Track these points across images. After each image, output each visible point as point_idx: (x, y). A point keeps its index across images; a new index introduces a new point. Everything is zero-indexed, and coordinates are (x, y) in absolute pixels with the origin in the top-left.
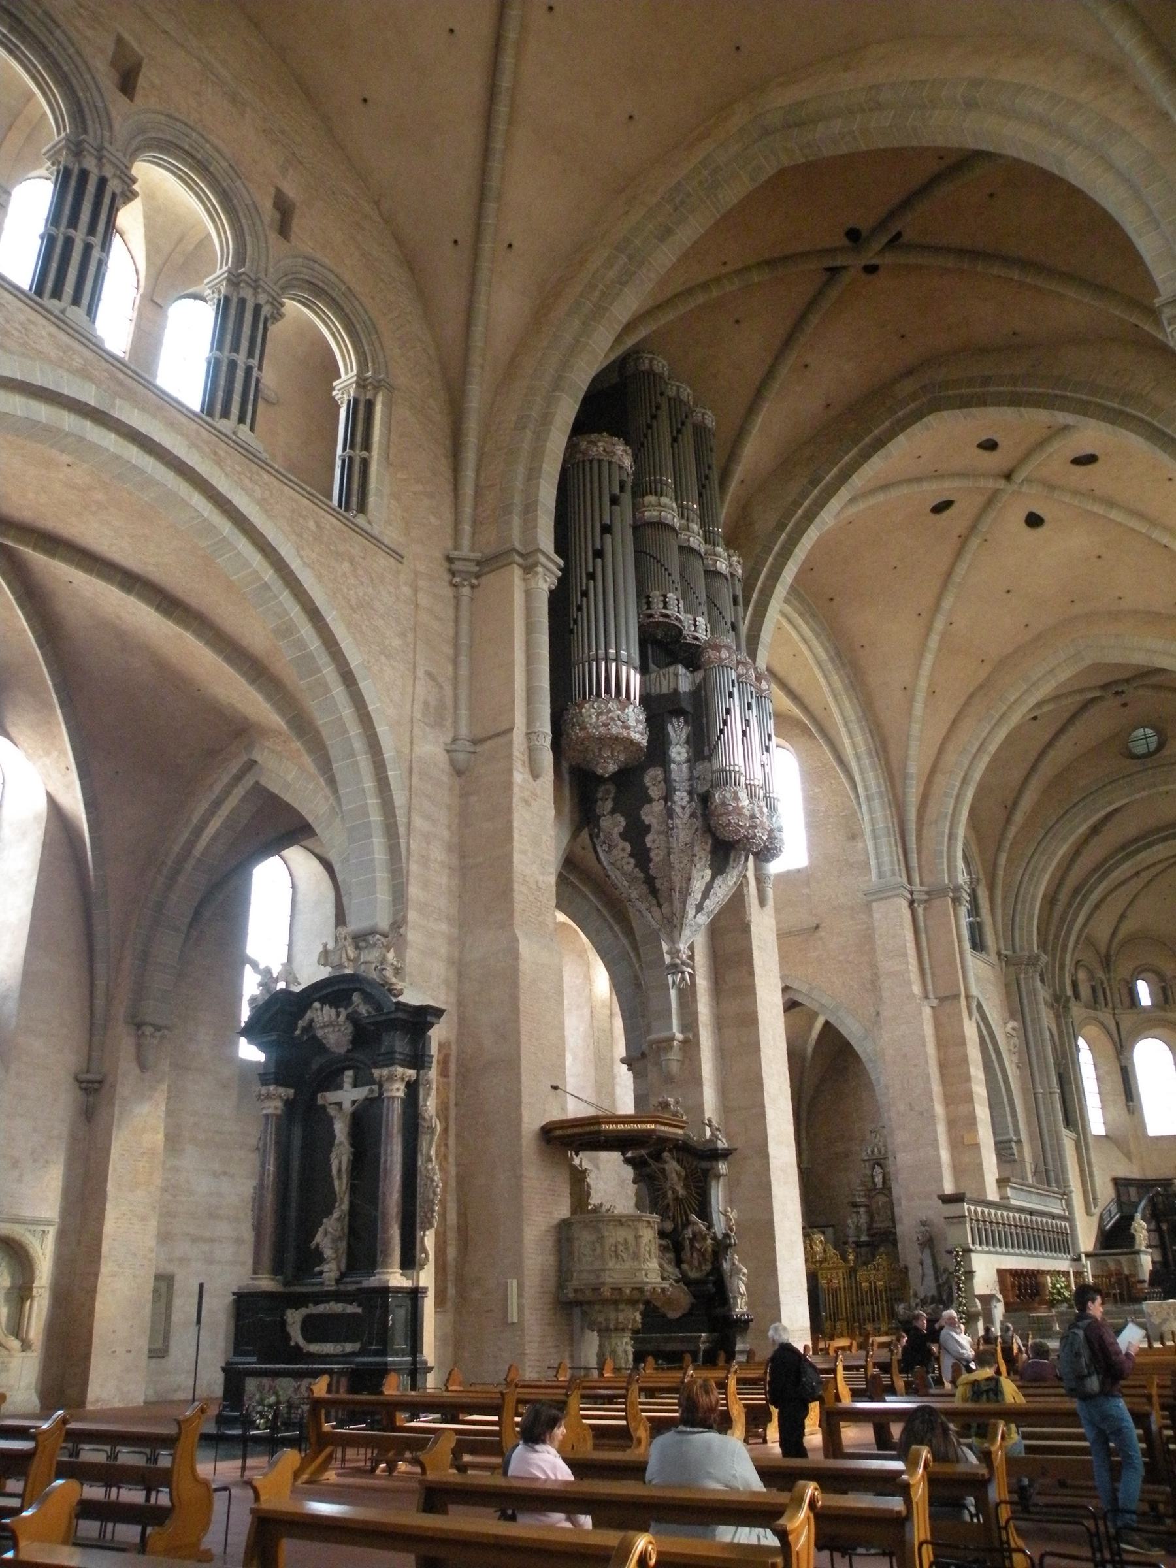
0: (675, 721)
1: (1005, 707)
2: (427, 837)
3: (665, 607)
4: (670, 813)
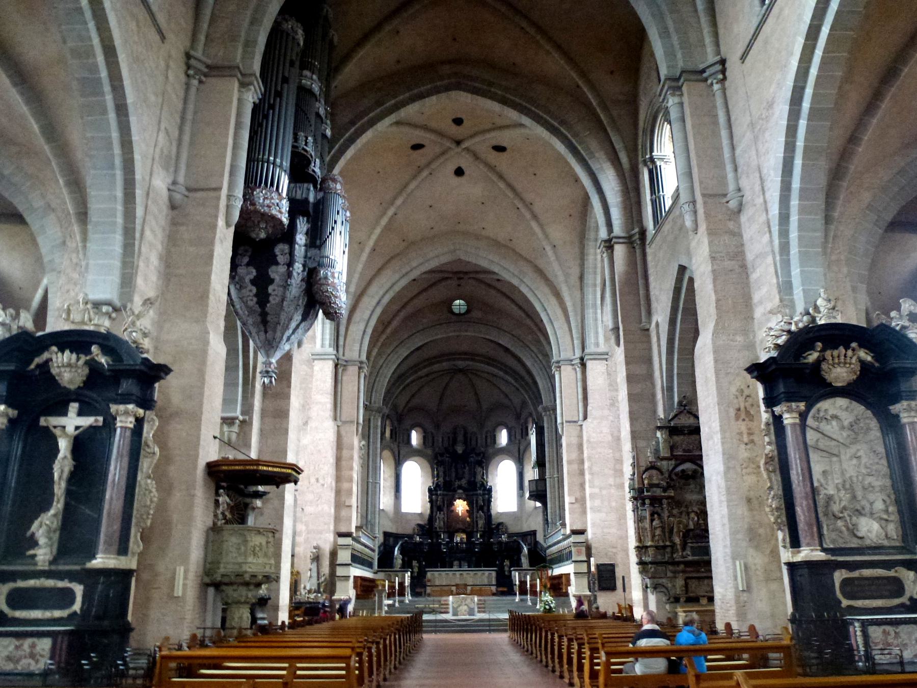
0: (301, 218)
1: (409, 269)
2: (151, 245)
3: (306, 145)
4: (289, 275)
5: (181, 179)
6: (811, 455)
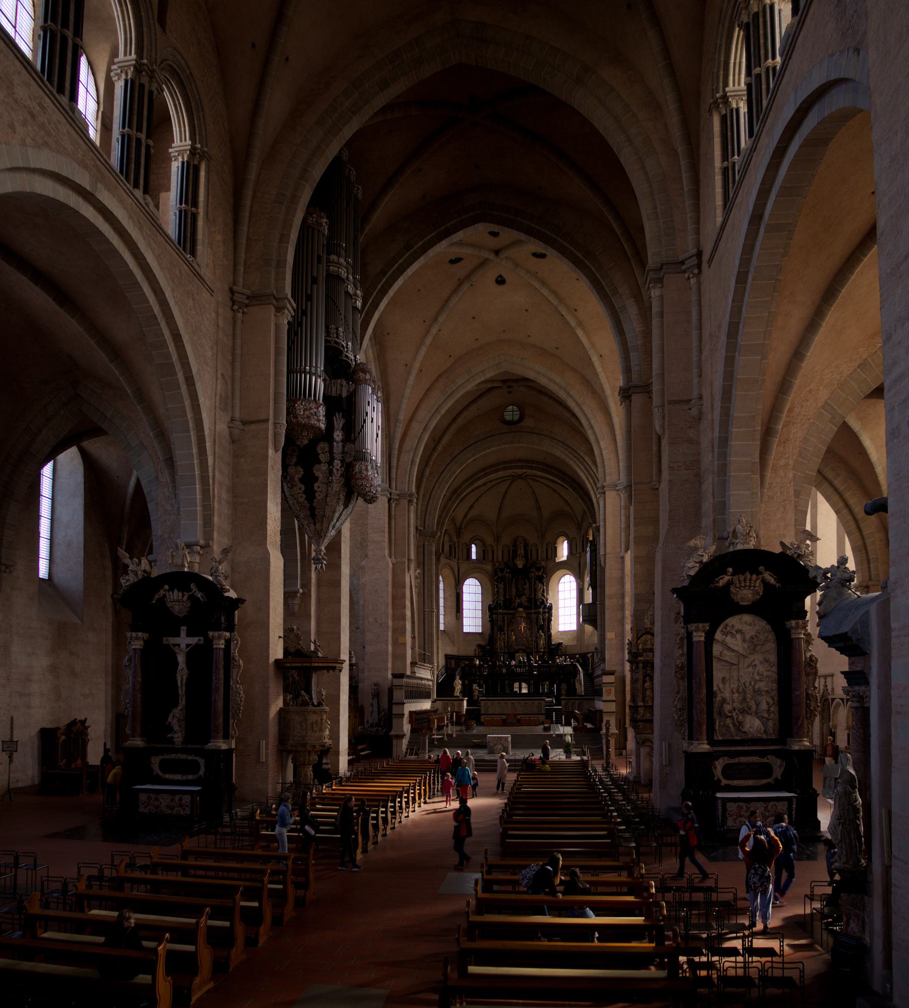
0: (337, 414)
4: (331, 473)
5: (237, 415)
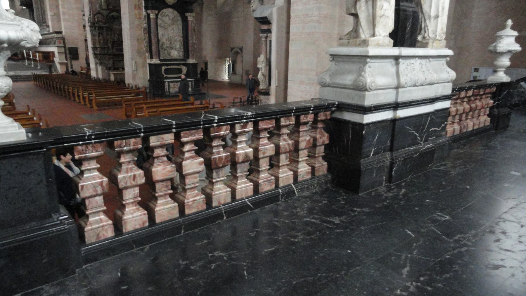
6: (159, 28)
